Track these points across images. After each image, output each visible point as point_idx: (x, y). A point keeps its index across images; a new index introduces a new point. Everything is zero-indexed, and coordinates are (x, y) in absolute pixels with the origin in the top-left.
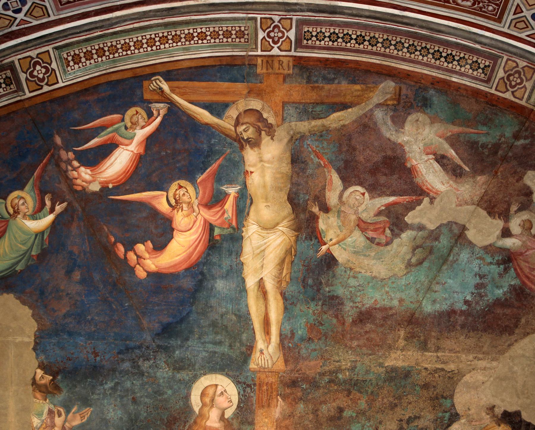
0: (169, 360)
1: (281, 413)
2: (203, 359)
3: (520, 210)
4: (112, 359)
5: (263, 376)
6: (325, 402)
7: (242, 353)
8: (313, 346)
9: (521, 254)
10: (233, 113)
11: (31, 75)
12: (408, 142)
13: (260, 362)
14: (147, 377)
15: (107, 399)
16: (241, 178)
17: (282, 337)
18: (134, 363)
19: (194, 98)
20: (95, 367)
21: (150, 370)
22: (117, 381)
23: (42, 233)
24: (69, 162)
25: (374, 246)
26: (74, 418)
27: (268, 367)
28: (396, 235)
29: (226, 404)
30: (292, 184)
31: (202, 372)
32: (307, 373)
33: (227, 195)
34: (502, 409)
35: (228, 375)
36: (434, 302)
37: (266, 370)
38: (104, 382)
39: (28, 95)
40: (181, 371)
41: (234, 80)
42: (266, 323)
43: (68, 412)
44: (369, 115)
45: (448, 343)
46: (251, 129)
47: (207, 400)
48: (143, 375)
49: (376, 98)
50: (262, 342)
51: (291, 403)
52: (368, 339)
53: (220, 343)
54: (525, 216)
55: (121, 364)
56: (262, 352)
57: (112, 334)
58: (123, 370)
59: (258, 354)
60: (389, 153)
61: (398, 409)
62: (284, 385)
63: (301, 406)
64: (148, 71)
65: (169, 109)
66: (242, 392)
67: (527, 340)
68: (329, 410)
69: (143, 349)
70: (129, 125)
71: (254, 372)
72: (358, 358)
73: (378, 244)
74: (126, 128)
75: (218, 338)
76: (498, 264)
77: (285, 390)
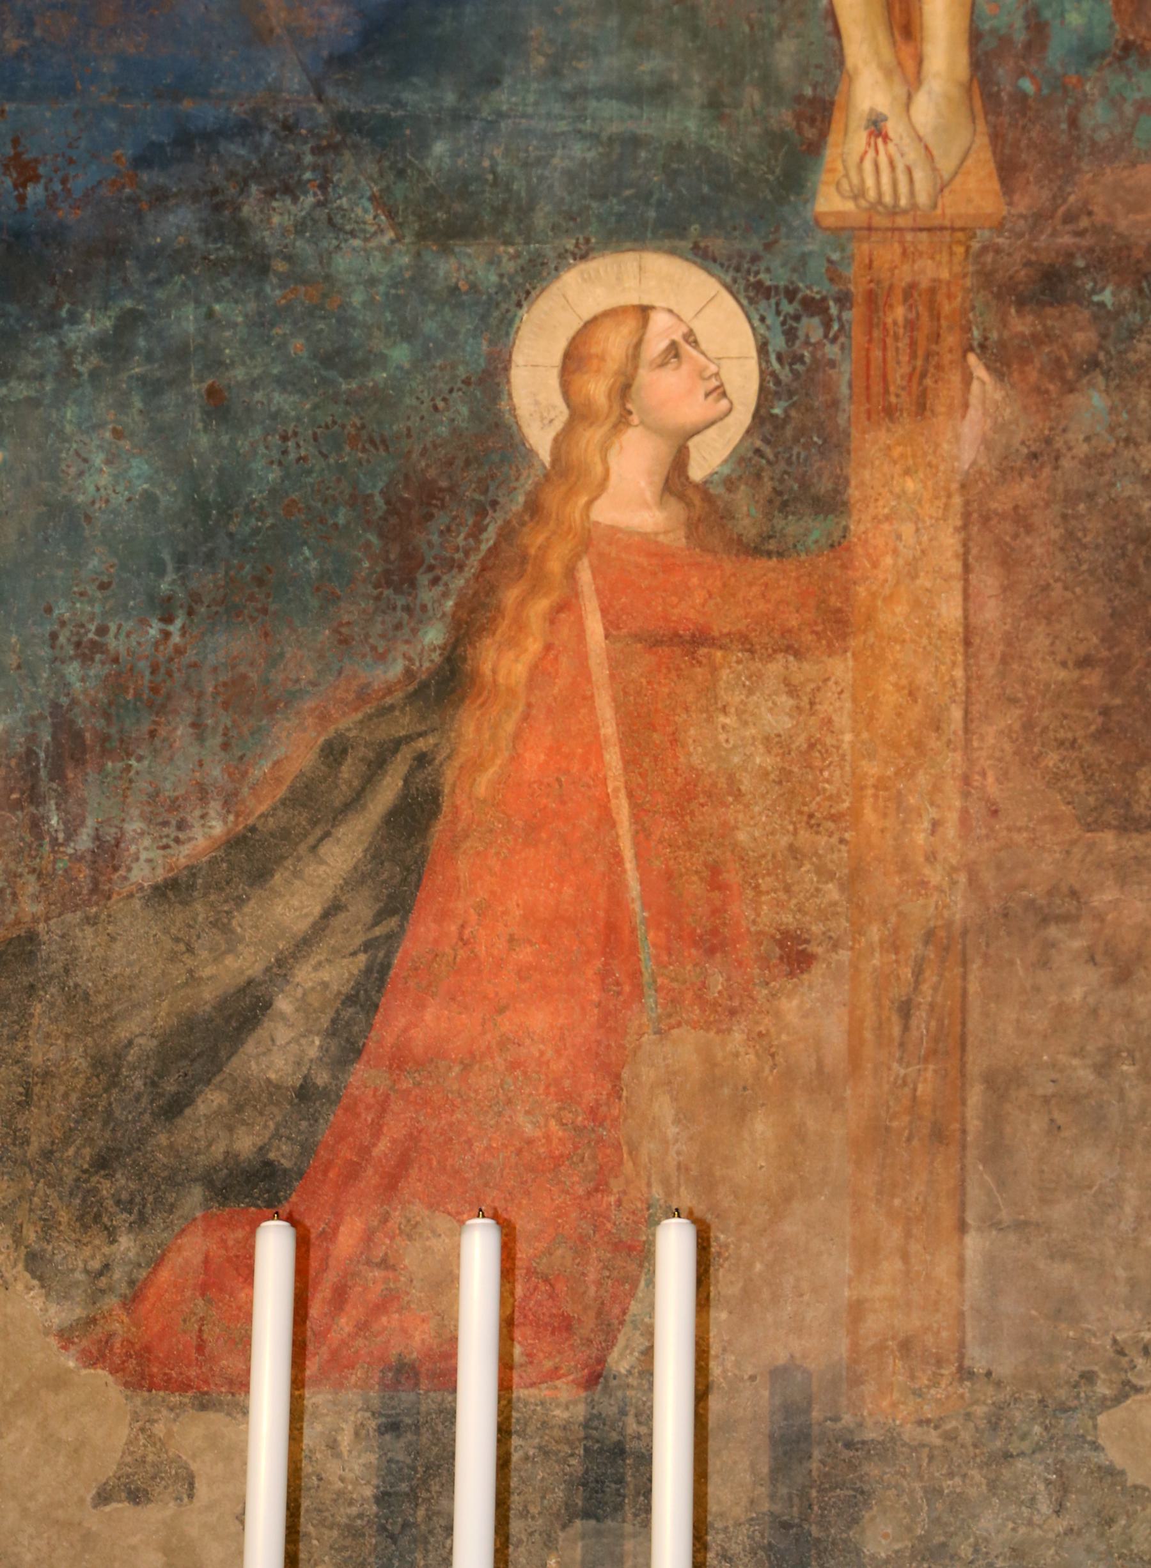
0: (400, 190)
1: (987, 444)
2: (571, 177)
4: (104, 191)
5: (887, 254)
7: (775, 139)
13: (870, 182)
14: (284, 280)
15: (78, 402)
18: (217, 208)
20: (19, 234)
21: (301, 246)
22: (128, 303)
27: (914, 206)
29: (694, 409)
31: (570, 244)
32: (1122, 224)
35: (702, 257)
37: (901, 221)
38: (64, 313)
40: (458, 246)
48: (264, 270)
50: (879, 76)
51: (1038, 390)
55: (150, 217)
56: (877, 128)
57: (108, 67)
58: (162, 248)
59: (859, 139)
62: (999, 296)
66: (778, 343)
69: (267, 139)
75: (646, 66)
77: (1004, 323)
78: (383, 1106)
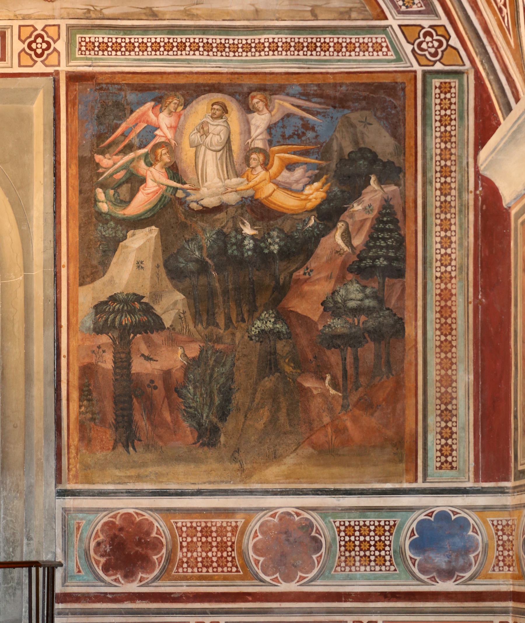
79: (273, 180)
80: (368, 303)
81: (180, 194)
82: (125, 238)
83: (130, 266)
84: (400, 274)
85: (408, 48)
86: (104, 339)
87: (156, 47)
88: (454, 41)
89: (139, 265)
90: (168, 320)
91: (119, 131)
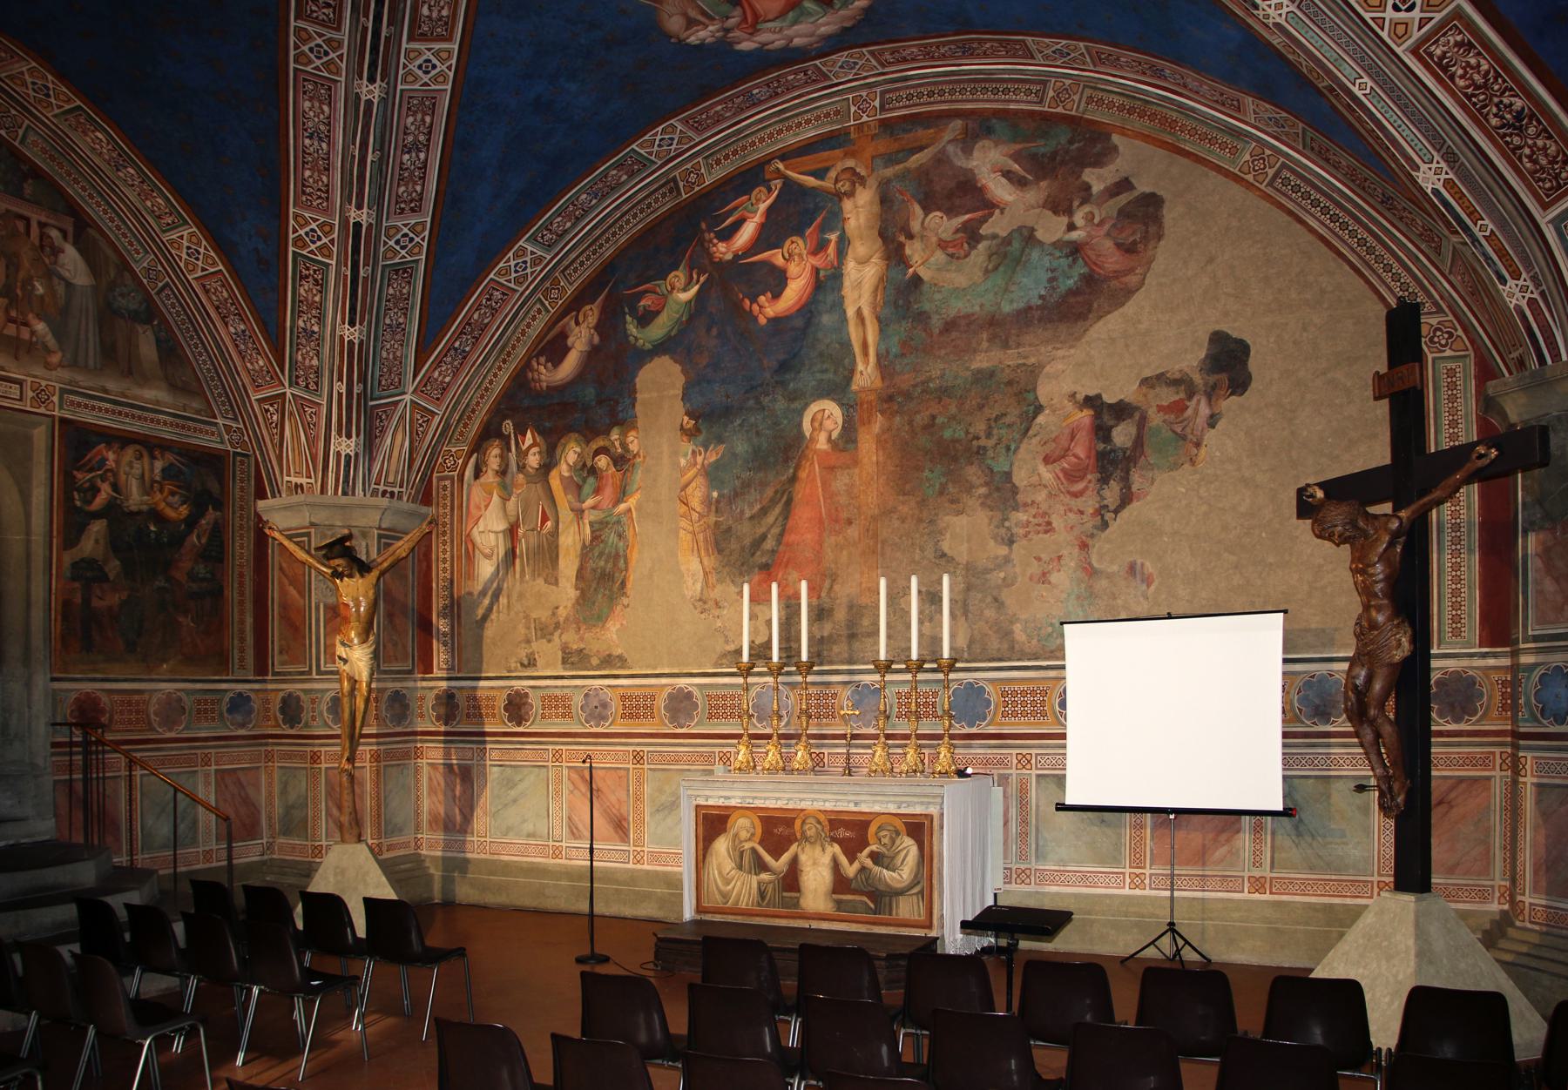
1: (880, 428)
3: (1081, 204)
5: (863, 396)
6: (918, 412)
8: (906, 361)
9: (1087, 244)
10: (833, 174)
11: (687, 182)
12: (976, 166)
16: (840, 226)
17: (879, 356)
19: (802, 170)
23: (690, 301)
24: (711, 241)
25: (954, 260)
26: (711, 455)
28: (973, 247)
29: (832, 427)
30: (882, 221)
33: (829, 241)
34: (1084, 394)
35: (833, 400)
36: (1012, 301)
39: (684, 197)
41: (833, 148)
42: (865, 346)
43: (706, 451)
44: (943, 151)
45: (1027, 338)
46: (848, 184)
47: (817, 425)
49: (947, 136)
52: (954, 347)
53: (825, 371)
54: (1087, 208)
56: (861, 373)
60: (962, 178)
61: (986, 409)
63: (898, 419)
64: (769, 158)
65: (784, 183)
67: (1101, 323)
68: (923, 419)
70: (754, 201)
71: (856, 393)
72: (946, 366)
73: (958, 258)
74: (752, 205)
76: (1067, 256)
78: (785, 553)
79: (164, 500)
80: (208, 576)
81: (118, 502)
82: (89, 524)
83: (92, 542)
84: (221, 560)
85: (226, 437)
86: (77, 585)
87: (107, 411)
88: (246, 438)
89: (97, 541)
90: (111, 576)
91: (88, 457)
